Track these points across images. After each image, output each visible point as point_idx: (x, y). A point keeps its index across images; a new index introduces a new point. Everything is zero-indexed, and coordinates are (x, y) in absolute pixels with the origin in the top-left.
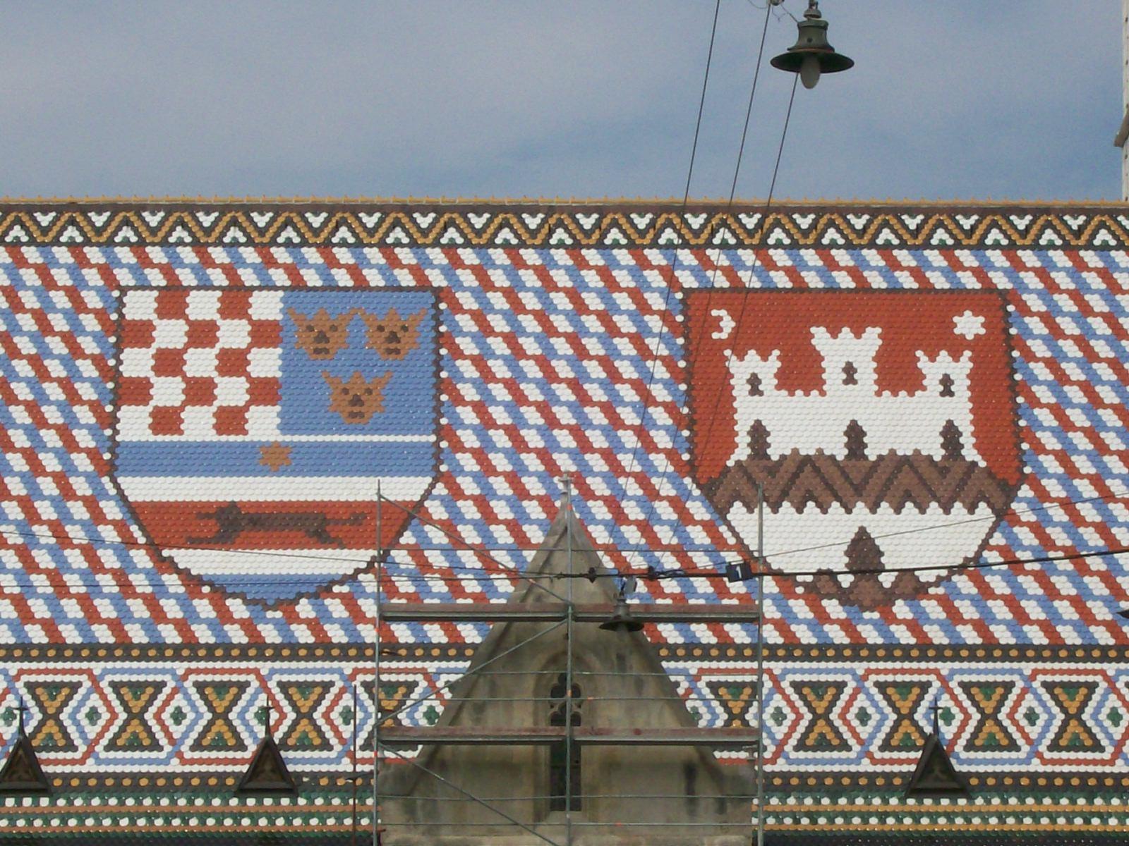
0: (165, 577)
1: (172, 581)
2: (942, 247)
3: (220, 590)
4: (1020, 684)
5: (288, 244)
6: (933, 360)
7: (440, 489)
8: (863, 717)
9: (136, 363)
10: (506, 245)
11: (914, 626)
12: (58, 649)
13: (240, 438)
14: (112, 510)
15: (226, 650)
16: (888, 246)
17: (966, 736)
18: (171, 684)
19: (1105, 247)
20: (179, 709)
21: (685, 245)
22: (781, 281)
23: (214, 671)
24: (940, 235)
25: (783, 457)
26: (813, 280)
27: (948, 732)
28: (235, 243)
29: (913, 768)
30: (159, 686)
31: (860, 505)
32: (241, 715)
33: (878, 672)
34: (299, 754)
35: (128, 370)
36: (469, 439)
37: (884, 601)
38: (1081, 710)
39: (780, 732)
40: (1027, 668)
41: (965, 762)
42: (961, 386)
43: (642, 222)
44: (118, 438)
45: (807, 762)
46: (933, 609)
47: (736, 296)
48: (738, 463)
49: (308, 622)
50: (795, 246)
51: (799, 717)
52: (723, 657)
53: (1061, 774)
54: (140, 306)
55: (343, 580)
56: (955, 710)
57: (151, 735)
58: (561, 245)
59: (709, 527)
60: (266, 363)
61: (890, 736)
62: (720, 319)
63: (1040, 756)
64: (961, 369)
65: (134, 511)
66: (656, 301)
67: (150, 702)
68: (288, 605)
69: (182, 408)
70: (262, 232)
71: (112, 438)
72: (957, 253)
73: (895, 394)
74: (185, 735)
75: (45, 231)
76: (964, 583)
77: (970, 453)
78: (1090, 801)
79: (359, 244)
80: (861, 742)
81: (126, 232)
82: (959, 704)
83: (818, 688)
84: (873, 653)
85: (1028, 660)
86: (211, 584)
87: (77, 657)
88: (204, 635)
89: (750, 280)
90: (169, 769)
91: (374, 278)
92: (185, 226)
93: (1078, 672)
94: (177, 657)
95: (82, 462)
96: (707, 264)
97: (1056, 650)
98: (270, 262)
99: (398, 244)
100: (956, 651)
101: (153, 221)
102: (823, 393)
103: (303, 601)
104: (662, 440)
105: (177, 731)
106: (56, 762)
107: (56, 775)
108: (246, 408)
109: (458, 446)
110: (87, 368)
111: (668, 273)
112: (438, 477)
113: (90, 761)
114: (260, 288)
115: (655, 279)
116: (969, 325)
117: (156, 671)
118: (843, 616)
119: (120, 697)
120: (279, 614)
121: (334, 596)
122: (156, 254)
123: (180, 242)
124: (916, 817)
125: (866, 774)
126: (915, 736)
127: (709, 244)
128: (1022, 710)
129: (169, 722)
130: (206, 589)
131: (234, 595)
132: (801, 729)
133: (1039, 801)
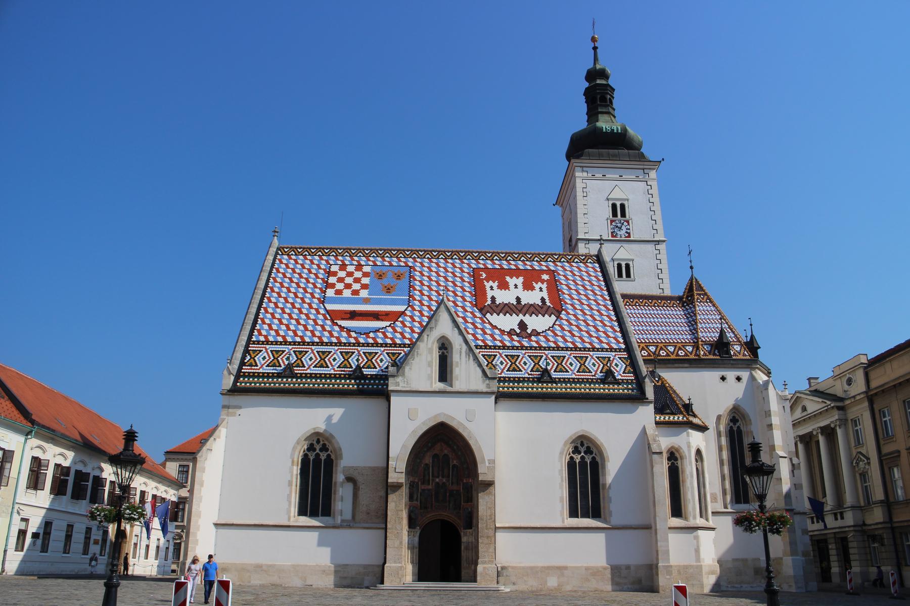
0: (334, 327)
1: (336, 328)
2: (537, 261)
3: (349, 331)
4: (567, 357)
5: (373, 256)
6: (537, 284)
7: (409, 308)
8: (525, 363)
9: (332, 280)
10: (428, 258)
11: (537, 342)
12: (303, 343)
13: (358, 296)
14: (322, 311)
15: (350, 344)
16: (523, 260)
17: (554, 368)
18: (333, 352)
19: (577, 262)
20: (335, 358)
21: (473, 259)
22: (498, 267)
23: (346, 349)
24: (536, 259)
25: (500, 303)
26: (505, 267)
27: (549, 368)
28: (360, 256)
29: (540, 376)
30: (330, 352)
31: (521, 315)
32: (352, 360)
33: (528, 353)
34: (367, 370)
35: (329, 281)
36: (417, 298)
37: (529, 336)
38: (585, 363)
39: (502, 367)
40: (569, 353)
41: (555, 375)
42: (545, 289)
43: (462, 254)
44: (326, 296)
45: (510, 374)
46: (542, 338)
47: (486, 269)
48: (488, 305)
49: (372, 338)
50: (500, 260)
51: (508, 363)
52: (486, 348)
53: (581, 378)
54: (334, 268)
55: (383, 328)
56: (550, 362)
57: (326, 364)
58: (442, 258)
59: (480, 318)
60: (366, 281)
61: (533, 368)
62: (482, 274)
63: (574, 374)
64: (544, 286)
65: (327, 311)
66: (466, 270)
67: (327, 356)
68: (367, 334)
69: (344, 289)
70: (367, 254)
71: (324, 296)
72: (541, 262)
73: (528, 291)
74: (336, 364)
75: (313, 253)
76: (549, 332)
77: (548, 304)
78: (590, 385)
79: (391, 257)
80: (525, 370)
81: (334, 254)
82: (551, 361)
83: (512, 356)
84: (527, 348)
85: (569, 351)
86: (346, 328)
87: (308, 345)
88: (343, 340)
89: (490, 266)
90: (331, 372)
91: (395, 264)
92: (348, 253)
93: (582, 354)
94: (336, 345)
95: (316, 301)
96: (479, 263)
97: (576, 348)
98: (369, 260)
99: (401, 257)
100: (549, 348)
101: (340, 251)
102: (509, 290)
103: (371, 333)
104: (468, 299)
105: (334, 363)
106: (299, 370)
107: (298, 373)
108: (360, 290)
109: (415, 299)
110: (320, 281)
111: (468, 264)
112: (409, 306)
113: (308, 370)
114: (365, 265)
115: (465, 265)
116: (545, 277)
117: (329, 349)
118: (518, 340)
119: (319, 355)
120: (364, 336)
121: (380, 332)
122: (340, 258)
123: (347, 256)
124: (542, 389)
125: (527, 378)
126: (540, 368)
127: (479, 259)
128: (568, 363)
129: (332, 361)
130: (345, 330)
131: (353, 331)
132: (508, 366)
133: (576, 385)
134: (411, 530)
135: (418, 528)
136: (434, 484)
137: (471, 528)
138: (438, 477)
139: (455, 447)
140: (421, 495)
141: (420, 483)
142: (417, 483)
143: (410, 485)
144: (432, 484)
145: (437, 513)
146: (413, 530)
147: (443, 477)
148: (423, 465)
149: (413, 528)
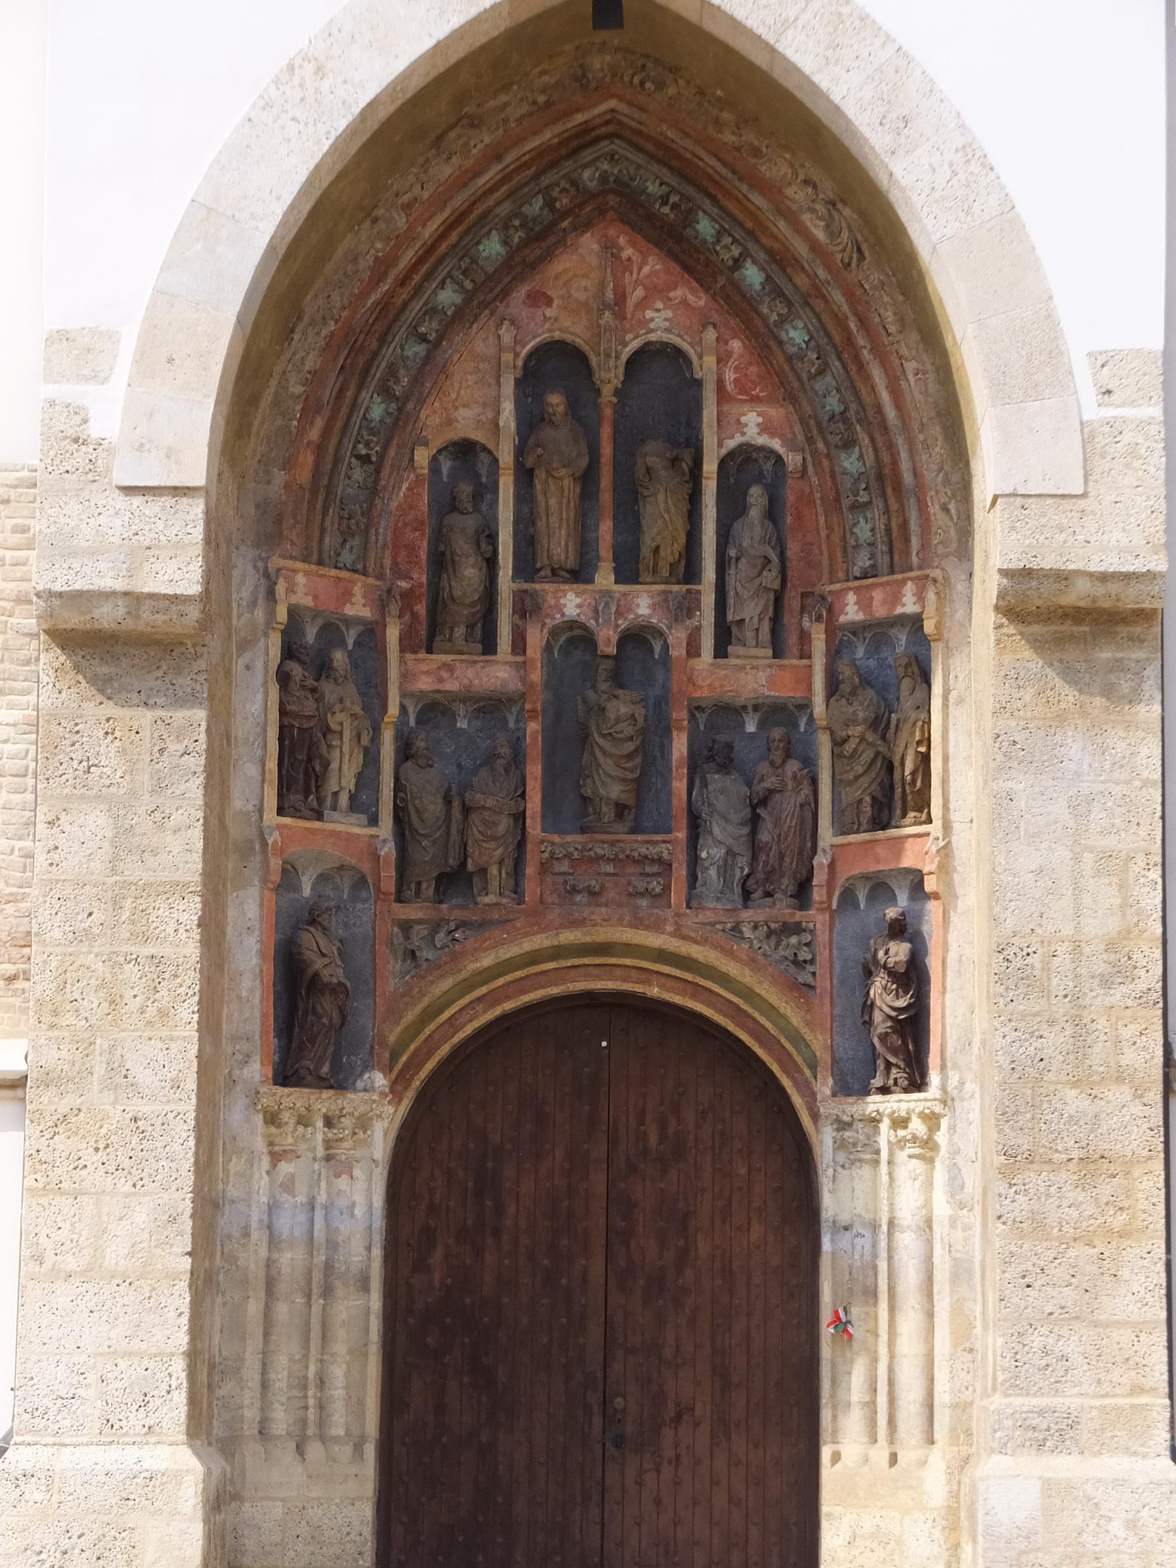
134: (293, 1098)
135: (379, 1080)
136: (536, 638)
137: (917, 1083)
138: (579, 574)
139: (752, 275)
140: (405, 752)
141: (393, 634)
142: (372, 634)
143: (289, 652)
144: (519, 644)
145: (568, 937)
146: (323, 1101)
147: (628, 572)
148: (422, 457)
149: (323, 1083)
